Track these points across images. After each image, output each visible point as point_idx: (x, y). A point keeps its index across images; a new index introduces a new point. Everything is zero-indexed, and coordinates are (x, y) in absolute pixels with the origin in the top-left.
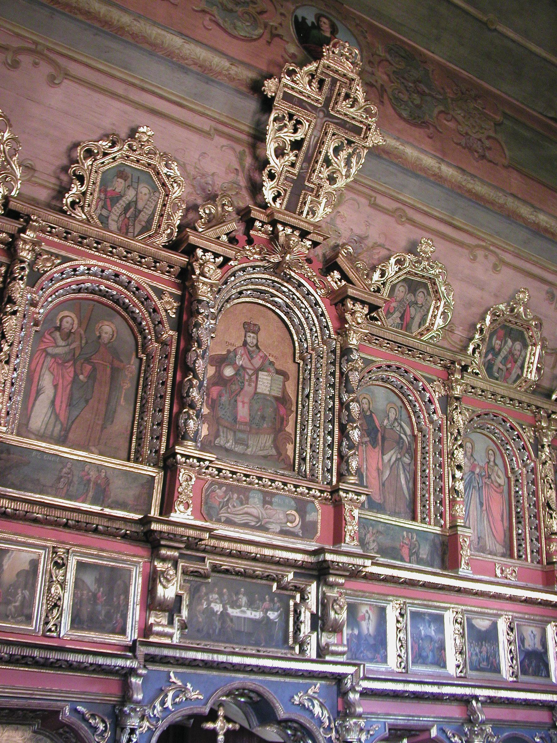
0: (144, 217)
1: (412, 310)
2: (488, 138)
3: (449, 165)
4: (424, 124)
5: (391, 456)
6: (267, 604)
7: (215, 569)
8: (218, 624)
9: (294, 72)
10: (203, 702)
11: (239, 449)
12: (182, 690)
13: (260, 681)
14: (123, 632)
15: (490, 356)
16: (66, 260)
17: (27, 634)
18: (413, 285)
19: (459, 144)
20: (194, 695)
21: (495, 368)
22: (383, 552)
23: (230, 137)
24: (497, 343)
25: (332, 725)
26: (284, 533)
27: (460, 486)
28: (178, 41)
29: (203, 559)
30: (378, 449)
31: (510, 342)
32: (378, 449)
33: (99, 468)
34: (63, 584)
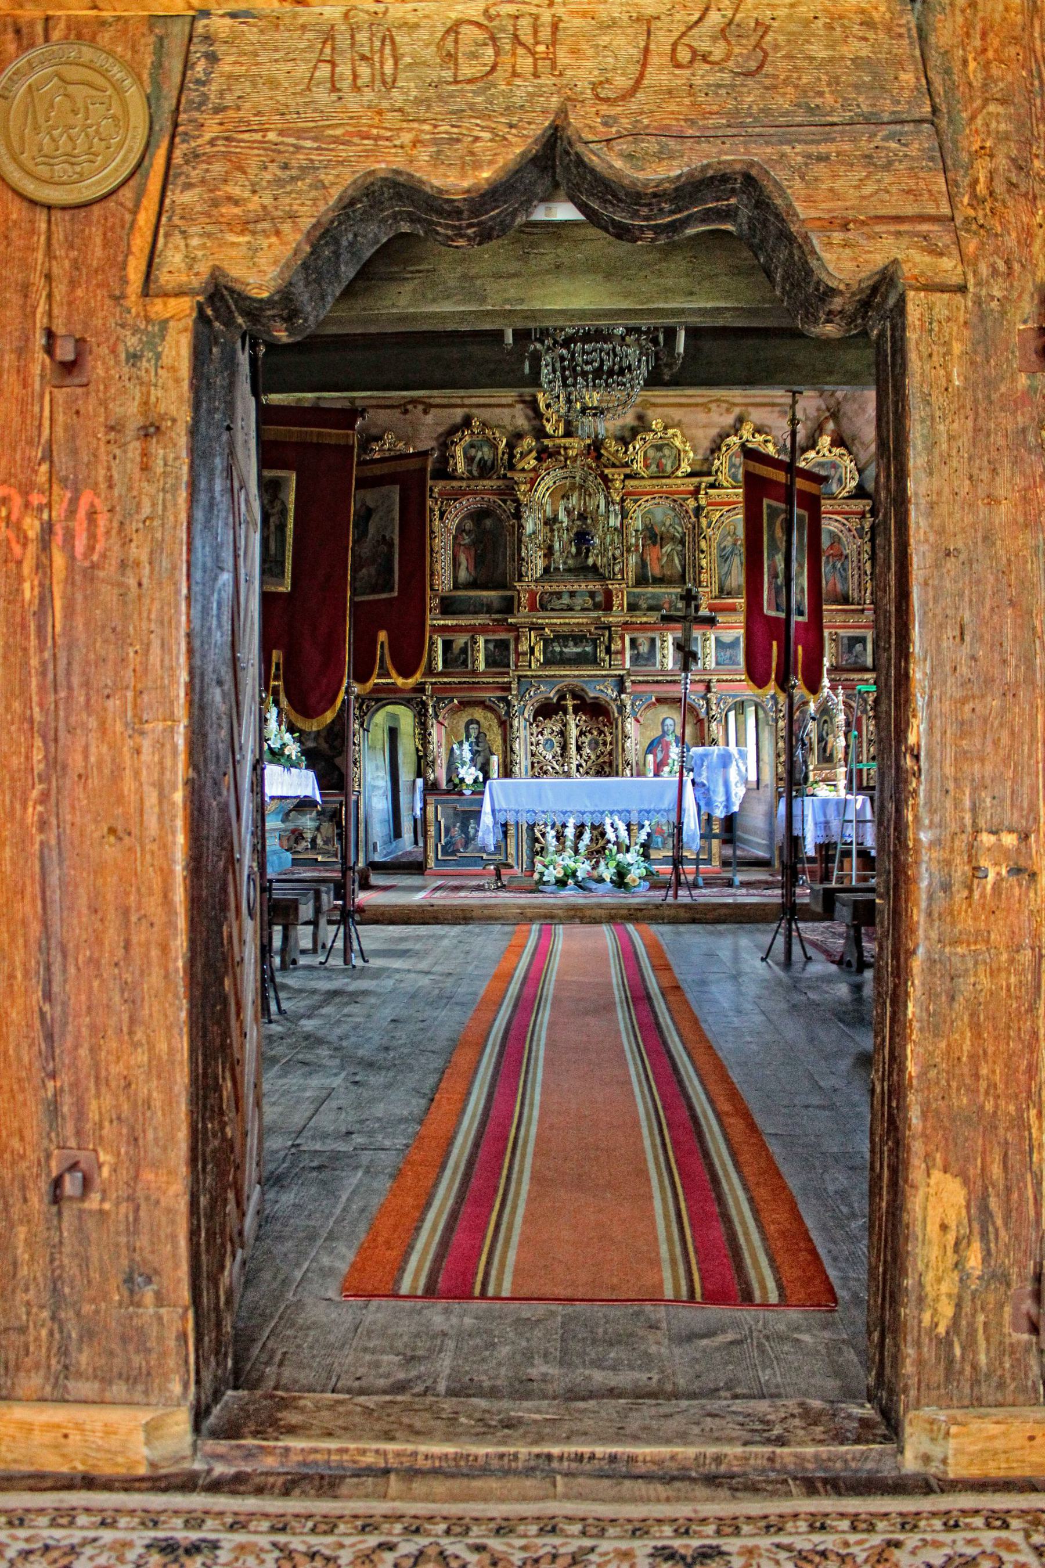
5: (668, 548)
18: (659, 448)
26: (583, 610)
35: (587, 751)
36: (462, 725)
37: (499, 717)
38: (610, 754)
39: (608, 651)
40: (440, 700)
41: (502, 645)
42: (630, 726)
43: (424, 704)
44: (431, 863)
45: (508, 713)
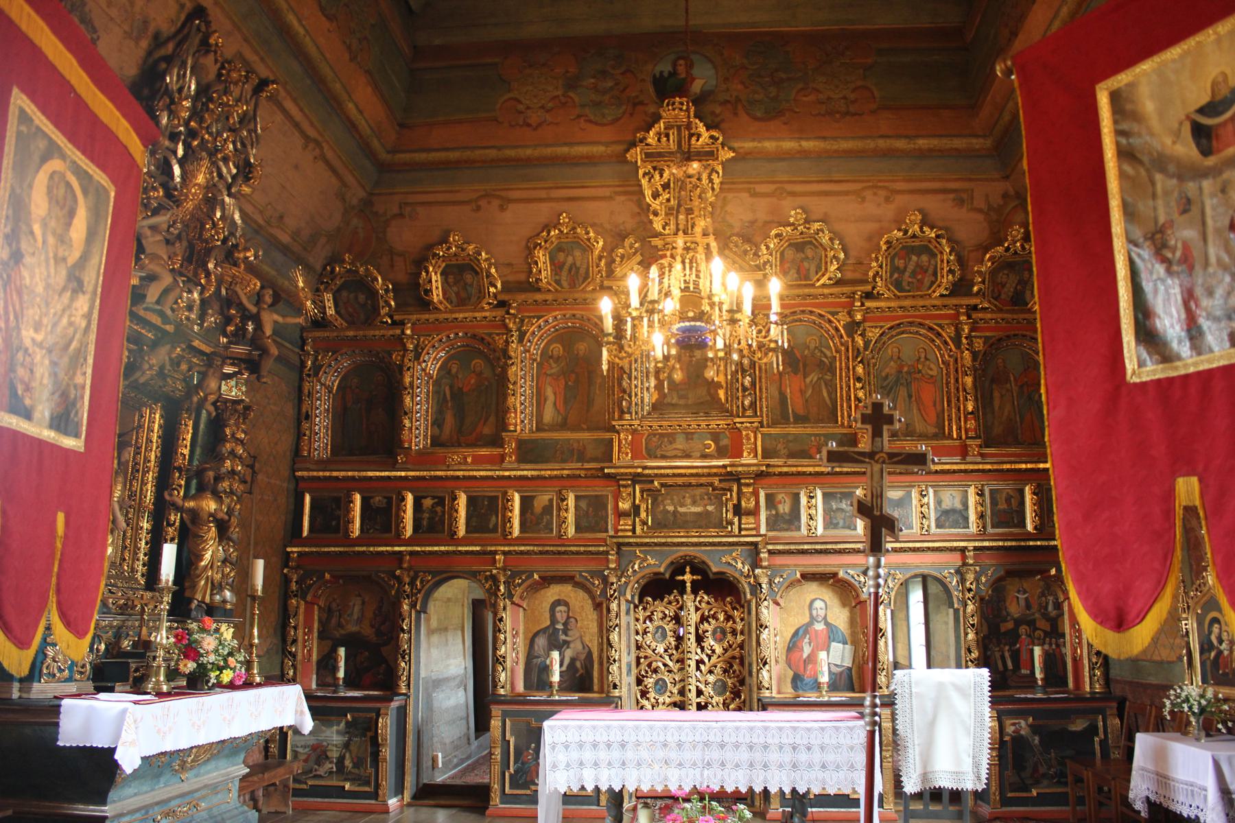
0: (582, 271)
1: (806, 264)
2: (854, 90)
3: (808, 139)
4: (780, 113)
5: (813, 377)
6: (706, 502)
7: (662, 485)
8: (672, 518)
9: (645, 138)
11: (682, 402)
12: (645, 560)
14: (607, 531)
15: (896, 276)
16: (539, 318)
17: (551, 538)
19: (819, 114)
20: (652, 562)
21: (905, 284)
22: (792, 455)
23: (625, 193)
24: (900, 263)
27: (861, 394)
28: (565, 150)
29: (652, 482)
30: (800, 375)
31: (914, 258)
32: (800, 375)
33: (578, 441)
34: (566, 510)
35: (710, 642)
36: (546, 606)
37: (593, 598)
38: (741, 646)
39: (738, 510)
40: (514, 575)
41: (598, 504)
42: (768, 613)
43: (494, 579)
44: (496, 799)
45: (604, 592)
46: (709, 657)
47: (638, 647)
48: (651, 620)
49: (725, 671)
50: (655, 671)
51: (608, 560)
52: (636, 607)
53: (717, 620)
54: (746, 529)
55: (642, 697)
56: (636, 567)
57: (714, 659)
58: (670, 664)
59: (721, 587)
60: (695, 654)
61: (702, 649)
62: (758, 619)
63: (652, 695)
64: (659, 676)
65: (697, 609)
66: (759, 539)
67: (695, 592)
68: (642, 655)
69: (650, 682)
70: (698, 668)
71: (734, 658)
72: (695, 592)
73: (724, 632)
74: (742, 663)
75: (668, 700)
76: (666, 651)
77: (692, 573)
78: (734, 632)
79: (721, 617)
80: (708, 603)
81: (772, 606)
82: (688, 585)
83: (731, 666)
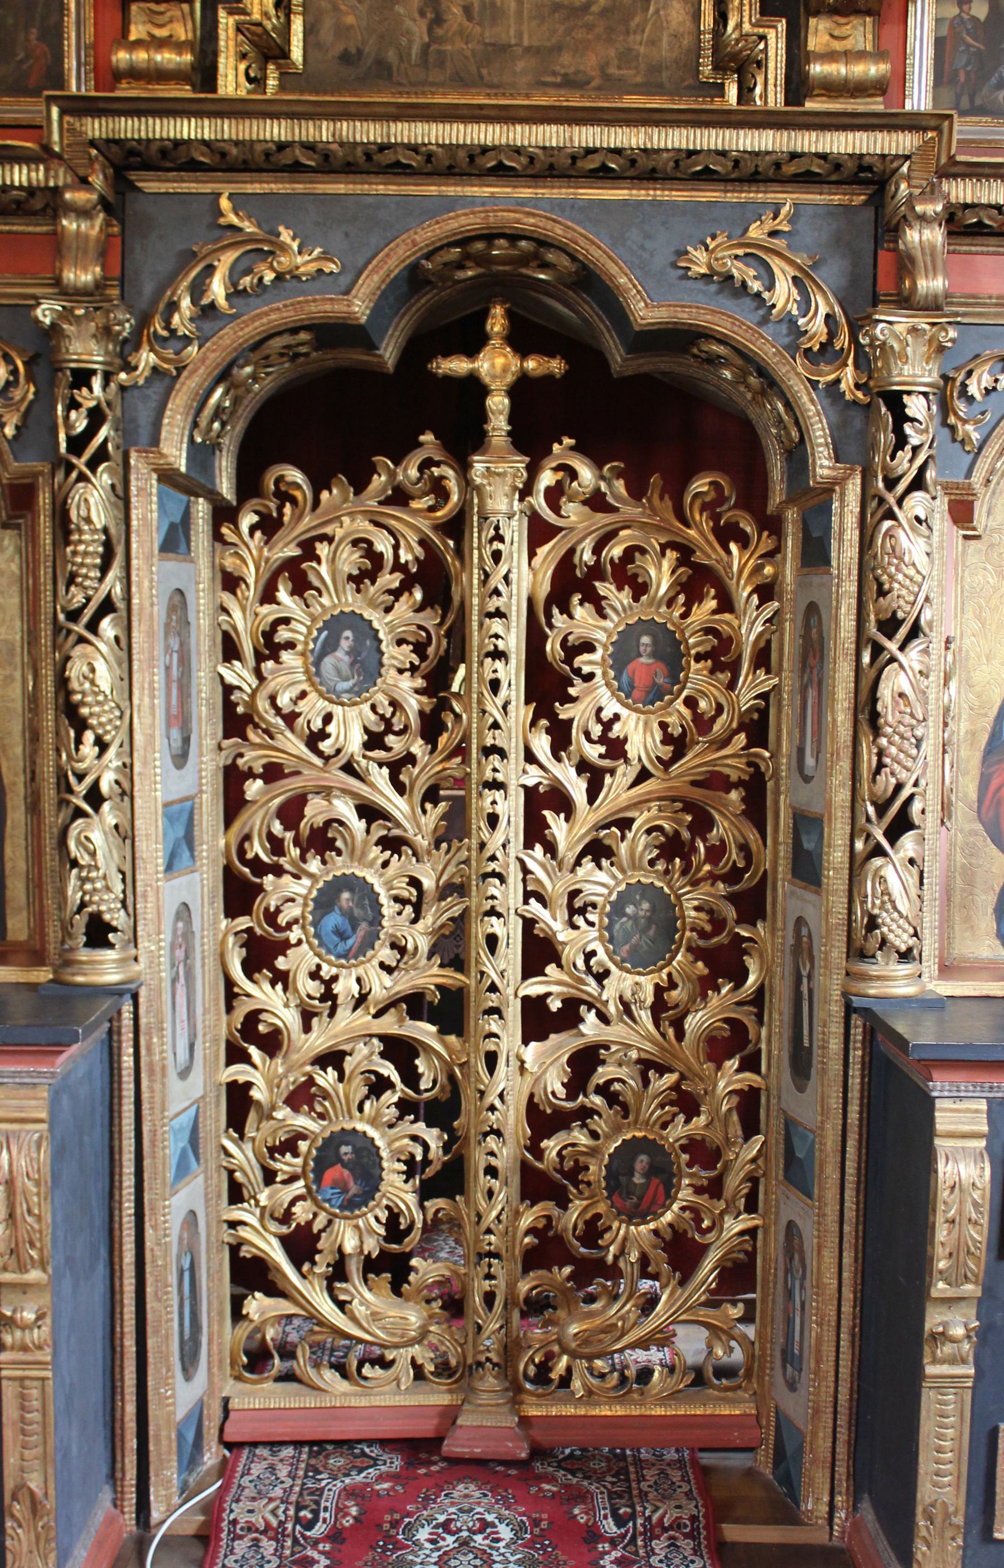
10: (344, 281)
12: (265, 249)
13: (560, 205)
20: (305, 263)
25: (843, 340)
35: (595, 699)
38: (757, 727)
46: (595, 778)
47: (236, 722)
48: (301, 587)
49: (672, 848)
50: (321, 841)
51: (56, 245)
52: (224, 514)
53: (639, 589)
54: (833, 88)
55: (250, 969)
56: (218, 289)
57: (618, 788)
58: (398, 805)
59: (658, 415)
60: (520, 753)
61: (561, 737)
62: (872, 584)
63: (298, 961)
64: (341, 866)
65: (540, 532)
66: (905, 142)
67: (530, 441)
68: (253, 758)
69: (290, 893)
70: (535, 832)
71: (715, 781)
72: (530, 441)
73: (671, 653)
74: (756, 811)
75: (382, 986)
76: (374, 741)
77: (522, 340)
78: (721, 655)
79: (662, 575)
80: (596, 502)
81: (941, 521)
82: (498, 403)
83: (703, 824)
